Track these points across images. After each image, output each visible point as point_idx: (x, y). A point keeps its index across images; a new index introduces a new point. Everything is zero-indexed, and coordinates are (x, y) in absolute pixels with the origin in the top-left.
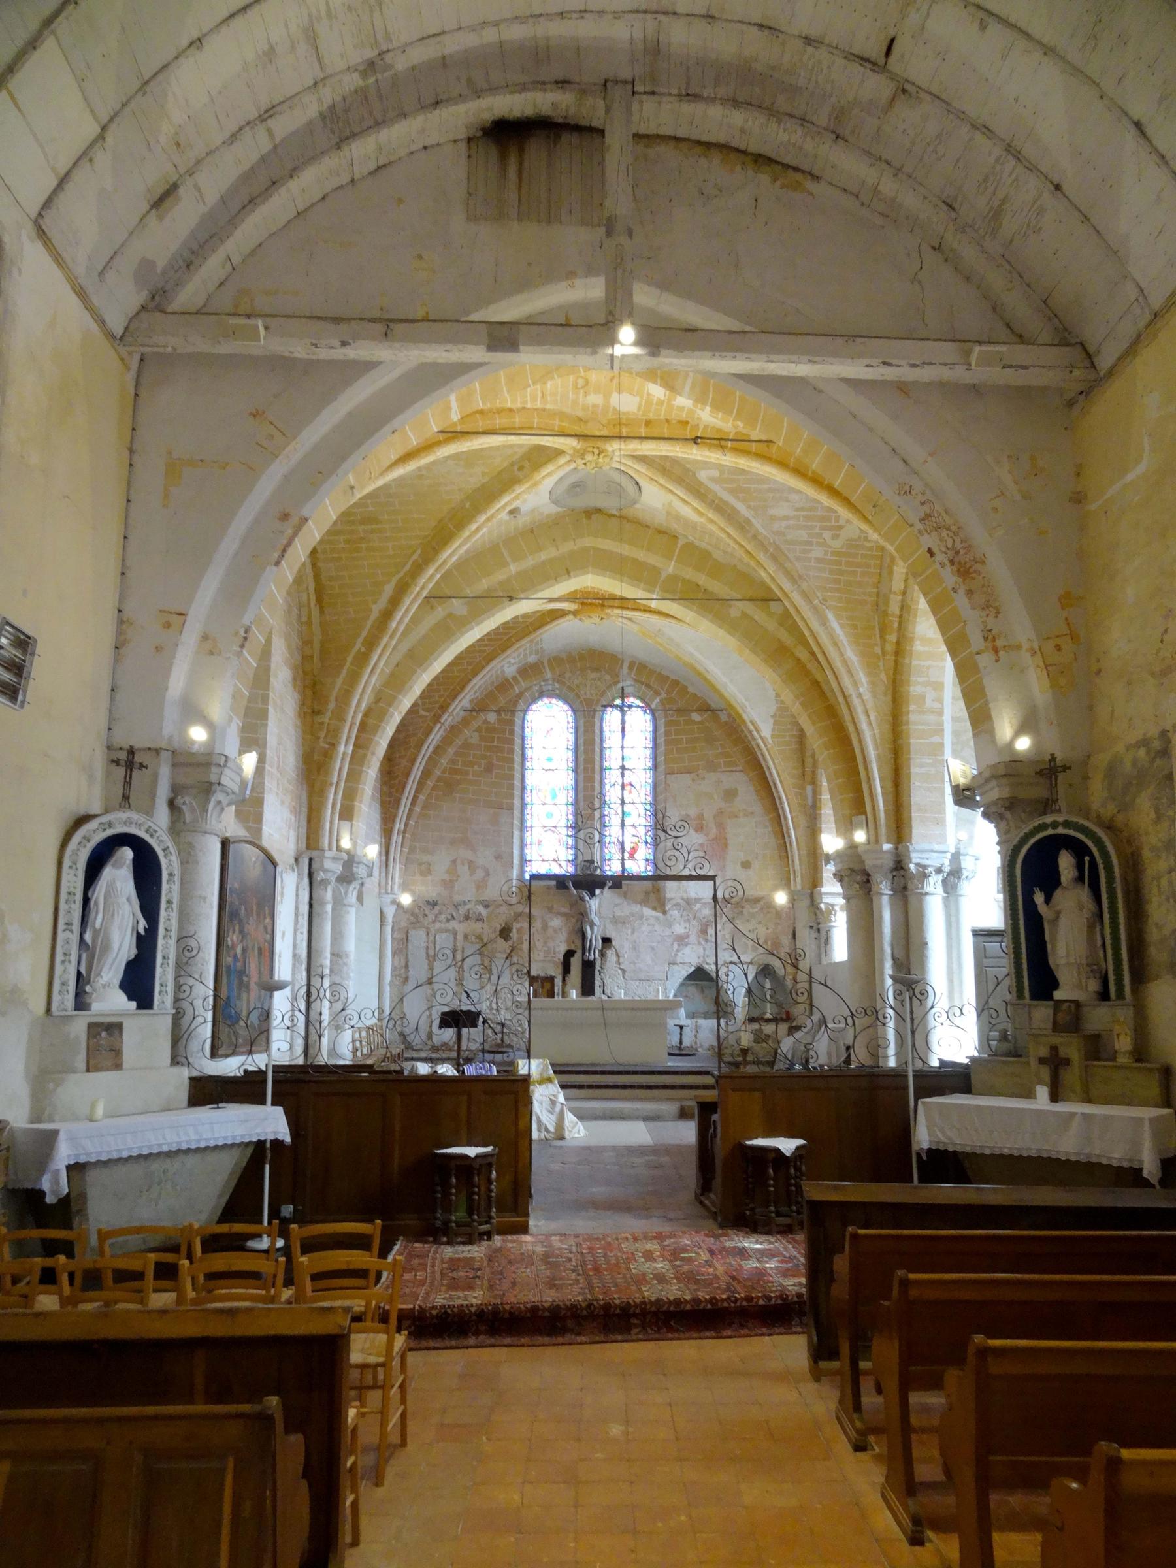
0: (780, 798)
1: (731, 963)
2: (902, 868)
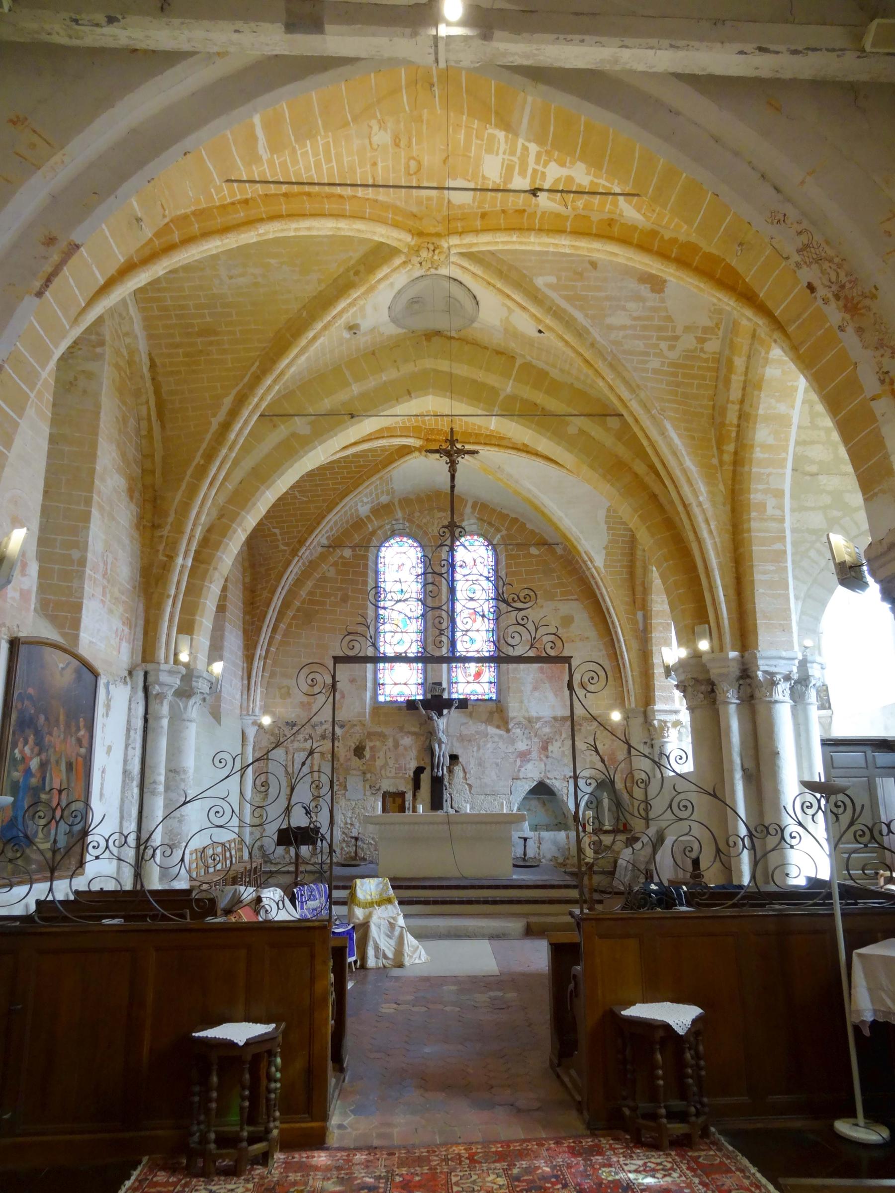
0: (613, 623)
2: (748, 677)
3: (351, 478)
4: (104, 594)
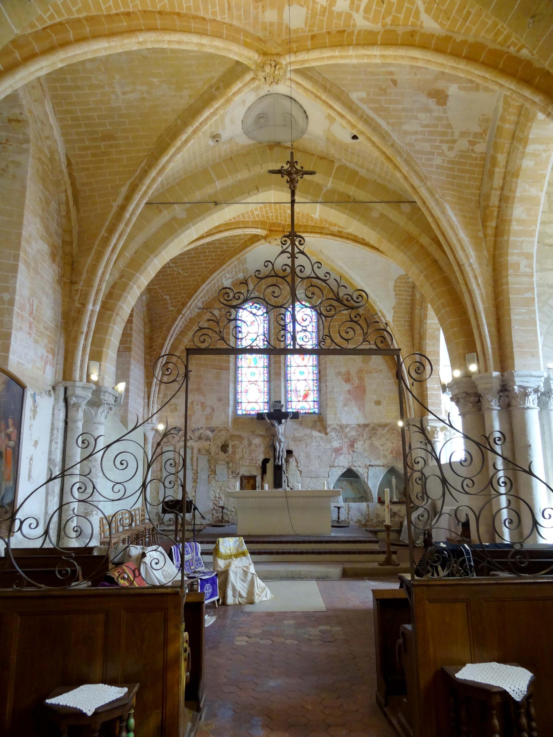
1: (370, 466)
2: (506, 390)
3: (219, 259)
4: (30, 327)
